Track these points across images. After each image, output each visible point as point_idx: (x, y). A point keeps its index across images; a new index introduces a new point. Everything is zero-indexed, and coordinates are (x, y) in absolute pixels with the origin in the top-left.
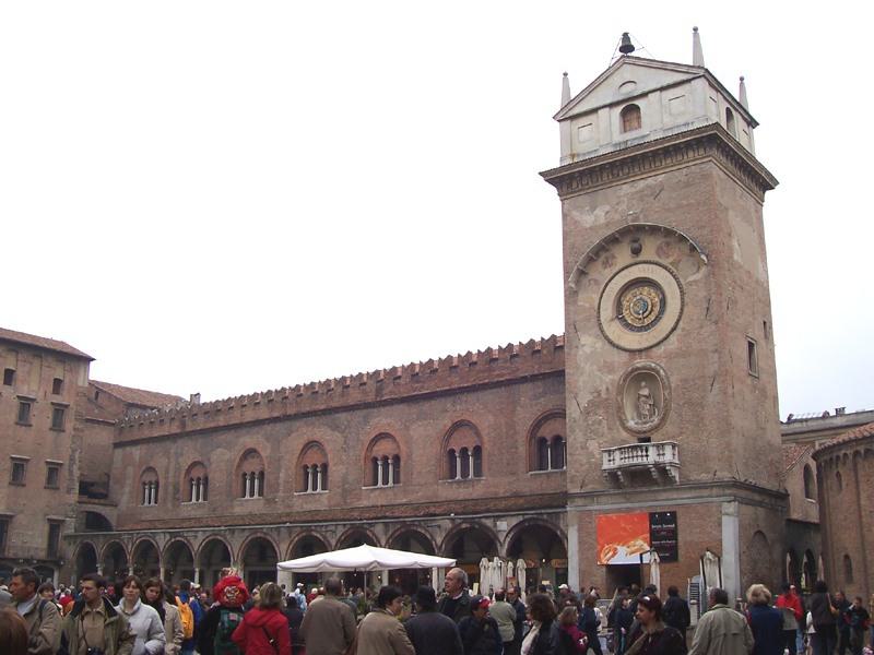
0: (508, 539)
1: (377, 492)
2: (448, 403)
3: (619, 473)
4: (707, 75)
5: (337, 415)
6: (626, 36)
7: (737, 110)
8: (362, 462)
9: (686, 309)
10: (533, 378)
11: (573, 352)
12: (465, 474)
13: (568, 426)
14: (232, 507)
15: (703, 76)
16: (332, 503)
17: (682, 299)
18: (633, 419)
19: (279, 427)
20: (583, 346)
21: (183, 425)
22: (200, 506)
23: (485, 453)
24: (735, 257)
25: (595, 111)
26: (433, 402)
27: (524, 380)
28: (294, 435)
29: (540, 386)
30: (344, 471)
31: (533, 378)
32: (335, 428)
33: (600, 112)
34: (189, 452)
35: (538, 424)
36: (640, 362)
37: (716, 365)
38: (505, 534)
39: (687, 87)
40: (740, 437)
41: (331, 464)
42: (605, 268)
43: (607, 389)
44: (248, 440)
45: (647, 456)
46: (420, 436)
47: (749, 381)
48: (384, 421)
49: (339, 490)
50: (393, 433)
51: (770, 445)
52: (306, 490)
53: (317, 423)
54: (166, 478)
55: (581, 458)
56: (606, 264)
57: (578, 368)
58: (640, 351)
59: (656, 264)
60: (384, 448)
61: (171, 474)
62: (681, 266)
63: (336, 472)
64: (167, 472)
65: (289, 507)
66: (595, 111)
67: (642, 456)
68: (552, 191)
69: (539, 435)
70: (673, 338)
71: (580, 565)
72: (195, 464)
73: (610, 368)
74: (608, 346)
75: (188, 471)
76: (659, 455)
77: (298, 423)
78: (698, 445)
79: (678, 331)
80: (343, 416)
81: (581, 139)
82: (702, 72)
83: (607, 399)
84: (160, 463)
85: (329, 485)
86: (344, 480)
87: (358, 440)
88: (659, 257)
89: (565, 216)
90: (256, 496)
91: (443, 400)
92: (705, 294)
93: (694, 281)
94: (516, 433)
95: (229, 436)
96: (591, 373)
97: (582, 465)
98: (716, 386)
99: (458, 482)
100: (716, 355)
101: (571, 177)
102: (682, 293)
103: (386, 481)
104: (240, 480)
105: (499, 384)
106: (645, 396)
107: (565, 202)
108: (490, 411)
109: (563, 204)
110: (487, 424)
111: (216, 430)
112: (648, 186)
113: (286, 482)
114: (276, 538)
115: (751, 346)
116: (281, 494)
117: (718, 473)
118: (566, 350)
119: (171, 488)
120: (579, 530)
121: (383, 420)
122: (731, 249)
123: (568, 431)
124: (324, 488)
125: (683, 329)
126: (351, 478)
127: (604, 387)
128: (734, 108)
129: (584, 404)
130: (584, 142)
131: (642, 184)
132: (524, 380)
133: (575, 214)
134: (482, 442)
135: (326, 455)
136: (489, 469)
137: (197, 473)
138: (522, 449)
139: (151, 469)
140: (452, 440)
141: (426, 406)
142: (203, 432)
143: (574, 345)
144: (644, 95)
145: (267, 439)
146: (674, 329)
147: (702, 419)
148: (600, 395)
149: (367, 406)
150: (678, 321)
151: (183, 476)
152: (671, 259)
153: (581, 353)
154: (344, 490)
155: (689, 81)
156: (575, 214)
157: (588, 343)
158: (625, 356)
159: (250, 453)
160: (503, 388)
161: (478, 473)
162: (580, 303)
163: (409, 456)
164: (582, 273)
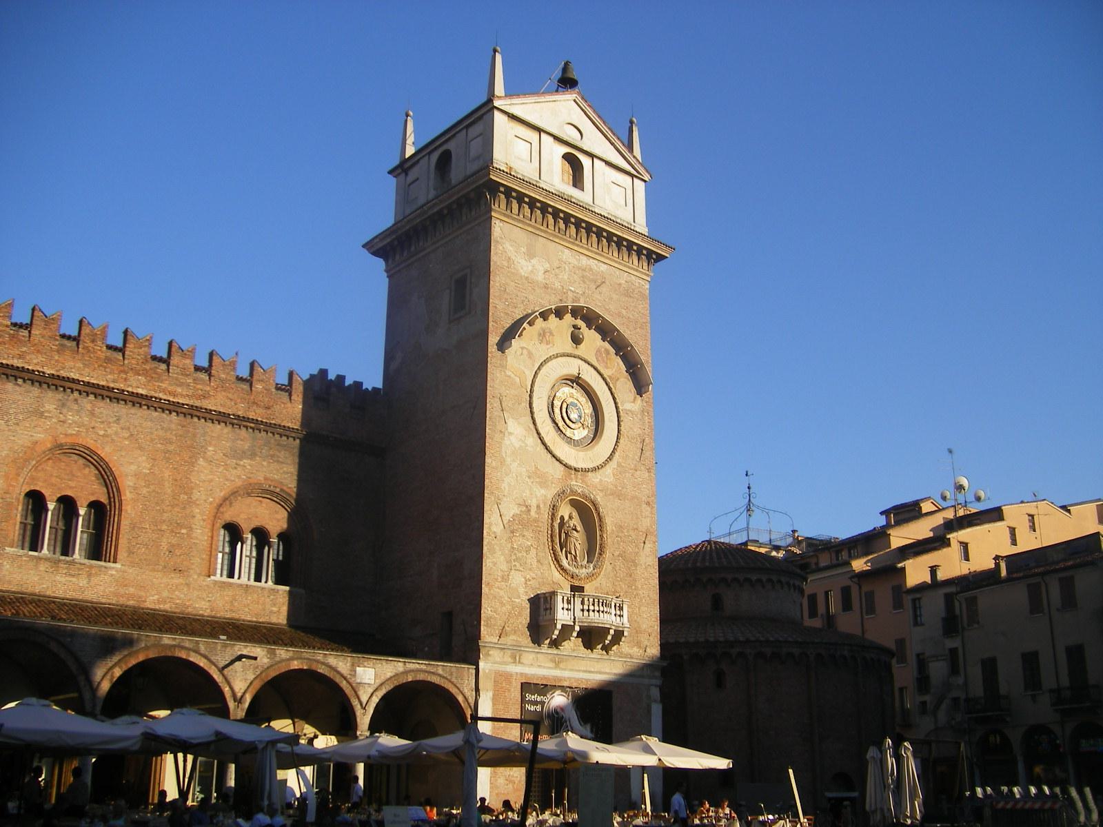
0: (375, 700)
2: (50, 400)
10: (239, 422)
11: (497, 436)
20: (510, 434)
27: (222, 418)
29: (244, 438)
31: (239, 422)
35: (227, 500)
36: (577, 484)
37: (648, 520)
38: (370, 690)
43: (538, 507)
55: (502, 593)
57: (503, 462)
70: (609, 470)
73: (539, 477)
83: (536, 520)
92: (640, 431)
94: (190, 502)
97: (502, 604)
98: (648, 545)
105: (172, 408)
108: (140, 448)
110: (133, 467)
117: (648, 650)
125: (619, 465)
131: (584, 261)
132: (222, 418)
136: (130, 552)
143: (499, 428)
148: (529, 511)
153: (507, 442)
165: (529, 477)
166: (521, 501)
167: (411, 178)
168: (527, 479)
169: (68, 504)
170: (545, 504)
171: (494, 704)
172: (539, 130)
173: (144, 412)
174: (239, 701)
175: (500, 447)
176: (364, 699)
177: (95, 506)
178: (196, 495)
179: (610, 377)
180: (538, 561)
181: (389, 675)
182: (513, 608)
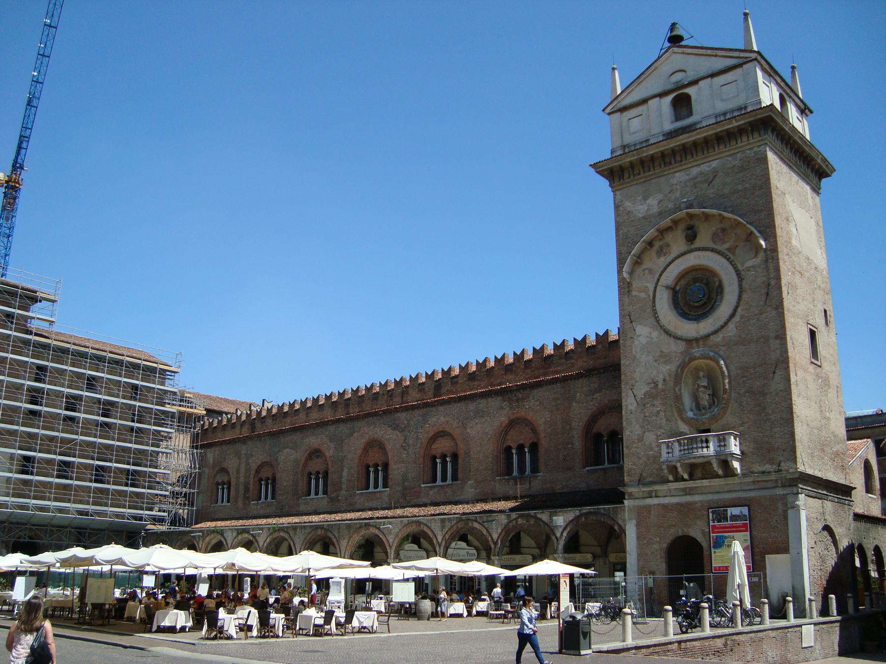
0: (565, 534)
1: (436, 489)
3: (678, 465)
4: (759, 58)
5: (399, 415)
7: (790, 97)
8: (421, 459)
9: (744, 296)
12: (522, 469)
13: (624, 419)
14: (298, 505)
15: (756, 59)
17: (740, 286)
18: (692, 410)
19: (343, 428)
21: (253, 428)
22: (269, 505)
23: (542, 451)
24: (794, 242)
25: (644, 101)
26: (490, 400)
30: (404, 469)
32: (395, 427)
33: (650, 102)
34: (257, 454)
35: (593, 419)
37: (778, 352)
38: (561, 530)
39: (739, 71)
40: (805, 427)
41: (391, 463)
42: (659, 256)
43: (664, 380)
44: (313, 440)
45: (707, 447)
47: (811, 368)
49: (400, 488)
50: (451, 431)
51: (835, 436)
52: (368, 488)
54: (238, 478)
56: (661, 252)
57: (634, 358)
58: (697, 340)
59: (713, 250)
60: (442, 446)
61: (242, 471)
62: (738, 251)
63: (396, 470)
64: (238, 473)
65: (351, 505)
66: (644, 101)
67: (702, 447)
68: (604, 183)
69: (595, 430)
70: (731, 326)
71: (639, 560)
72: (263, 465)
73: (664, 357)
74: (664, 337)
75: (258, 471)
76: (720, 446)
77: (358, 424)
78: (761, 434)
79: (737, 318)
80: (403, 416)
81: (632, 129)
82: (754, 56)
83: (664, 390)
84: (231, 464)
85: (390, 483)
86: (405, 478)
87: (417, 438)
88: (714, 242)
89: (617, 207)
90: (321, 495)
91: (500, 398)
92: (764, 279)
93: (753, 267)
95: (296, 437)
96: (646, 367)
97: (639, 458)
99: (515, 479)
100: (778, 342)
101: (622, 169)
102: (740, 278)
103: (444, 479)
104: (305, 479)
106: (704, 386)
107: (618, 193)
109: (615, 195)
111: (281, 432)
112: (701, 173)
113: (349, 481)
114: (337, 535)
115: (813, 334)
116: (343, 493)
117: (782, 464)
118: (621, 342)
119: (242, 488)
120: (638, 525)
121: (440, 419)
122: (789, 232)
123: (624, 423)
124: (385, 485)
125: (742, 317)
127: (661, 376)
128: (788, 94)
129: (640, 394)
130: (635, 133)
131: (695, 171)
133: (628, 204)
134: (538, 439)
135: (386, 454)
137: (266, 473)
138: (578, 444)
139: (224, 470)
140: (508, 437)
142: (272, 434)
143: (630, 335)
144: (695, 82)
146: (733, 315)
147: (765, 408)
149: (426, 405)
150: (737, 307)
151: (252, 476)
152: (727, 245)
153: (636, 343)
154: (405, 489)
155: (740, 65)
156: (628, 204)
157: (643, 332)
158: (681, 346)
159: (316, 453)
160: (558, 385)
161: (535, 469)
162: (634, 293)
163: (467, 454)
164: (638, 262)
165: (656, 361)
166: (650, 381)
168: (655, 363)
169: (520, 448)
170: (670, 376)
171: (638, 529)
173: (545, 388)
174: (496, 544)
175: (631, 349)
176: (558, 535)
178: (574, 423)
179: (728, 249)
180: (667, 420)
181: (571, 519)
182: (648, 459)
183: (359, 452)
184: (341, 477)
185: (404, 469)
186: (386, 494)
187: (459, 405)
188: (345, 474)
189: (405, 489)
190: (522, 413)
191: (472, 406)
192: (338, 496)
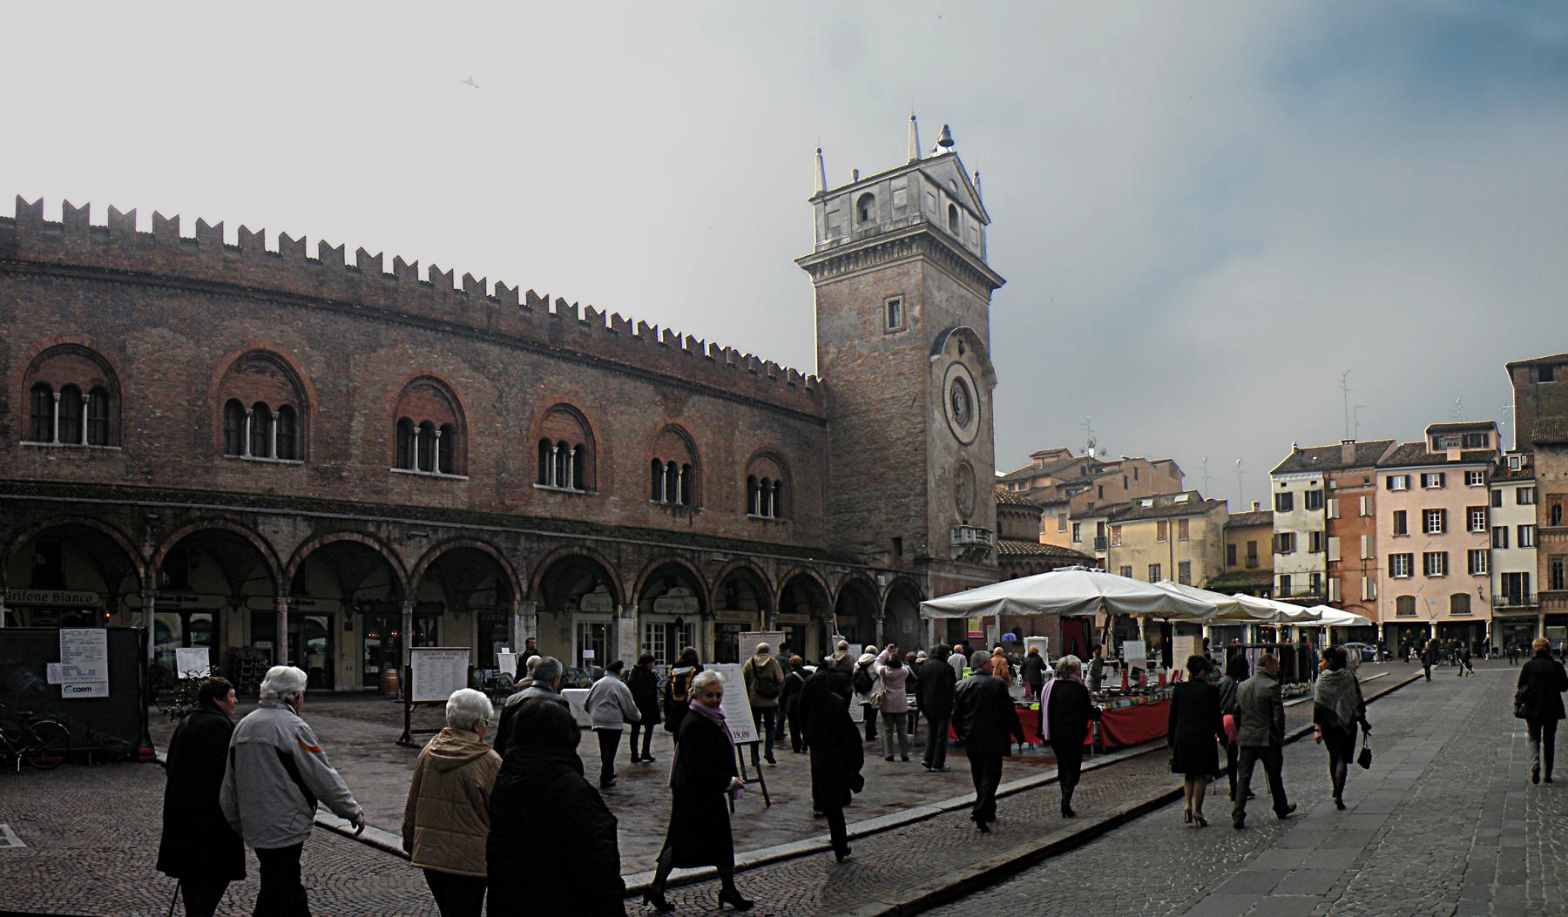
5: (485, 346)
6: (946, 130)
16: (477, 501)
28: (382, 352)
30: (499, 449)
32: (479, 368)
46: (630, 425)
48: (567, 385)
49: (492, 482)
53: (438, 347)
63: (482, 445)
65: (377, 493)
86: (501, 466)
87: (524, 402)
116: (354, 463)
121: (565, 382)
126: (511, 465)
141: (629, 385)
145: (312, 341)
154: (500, 483)
163: (608, 451)
167: (829, 208)
172: (938, 186)
177: (685, 467)
183: (395, 391)
184: (348, 430)
185: (499, 449)
186: (463, 485)
187: (593, 371)
188: (356, 425)
189: (500, 483)
190: (679, 421)
191: (615, 382)
192: (339, 469)
